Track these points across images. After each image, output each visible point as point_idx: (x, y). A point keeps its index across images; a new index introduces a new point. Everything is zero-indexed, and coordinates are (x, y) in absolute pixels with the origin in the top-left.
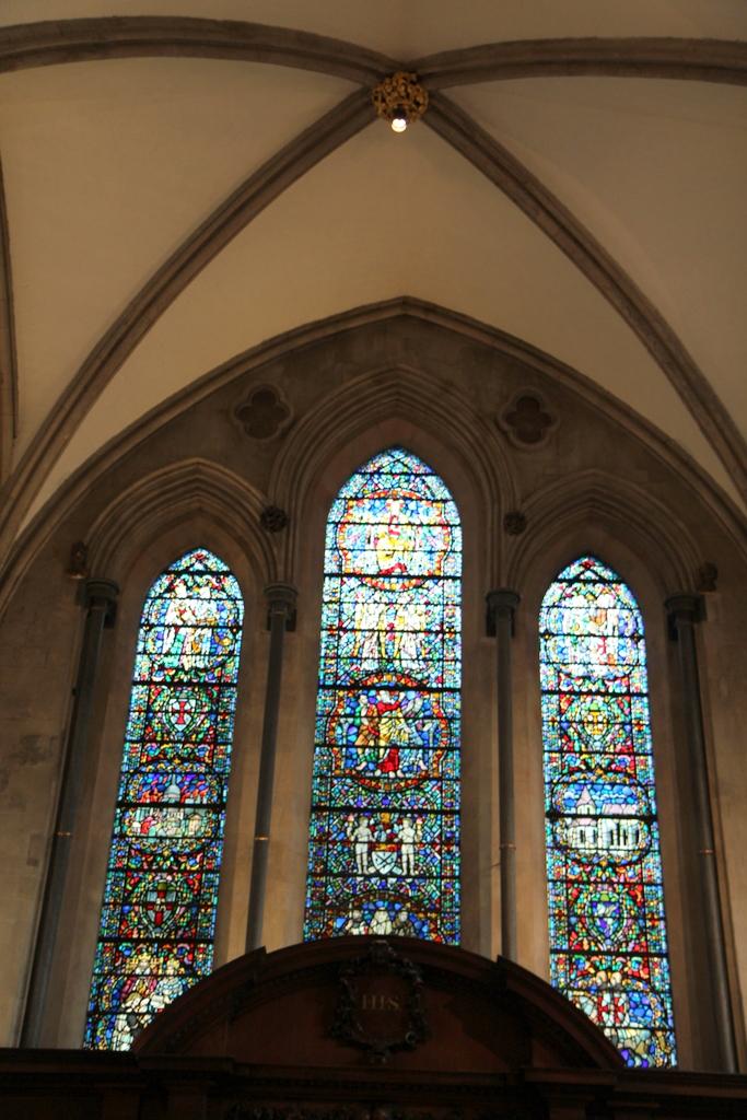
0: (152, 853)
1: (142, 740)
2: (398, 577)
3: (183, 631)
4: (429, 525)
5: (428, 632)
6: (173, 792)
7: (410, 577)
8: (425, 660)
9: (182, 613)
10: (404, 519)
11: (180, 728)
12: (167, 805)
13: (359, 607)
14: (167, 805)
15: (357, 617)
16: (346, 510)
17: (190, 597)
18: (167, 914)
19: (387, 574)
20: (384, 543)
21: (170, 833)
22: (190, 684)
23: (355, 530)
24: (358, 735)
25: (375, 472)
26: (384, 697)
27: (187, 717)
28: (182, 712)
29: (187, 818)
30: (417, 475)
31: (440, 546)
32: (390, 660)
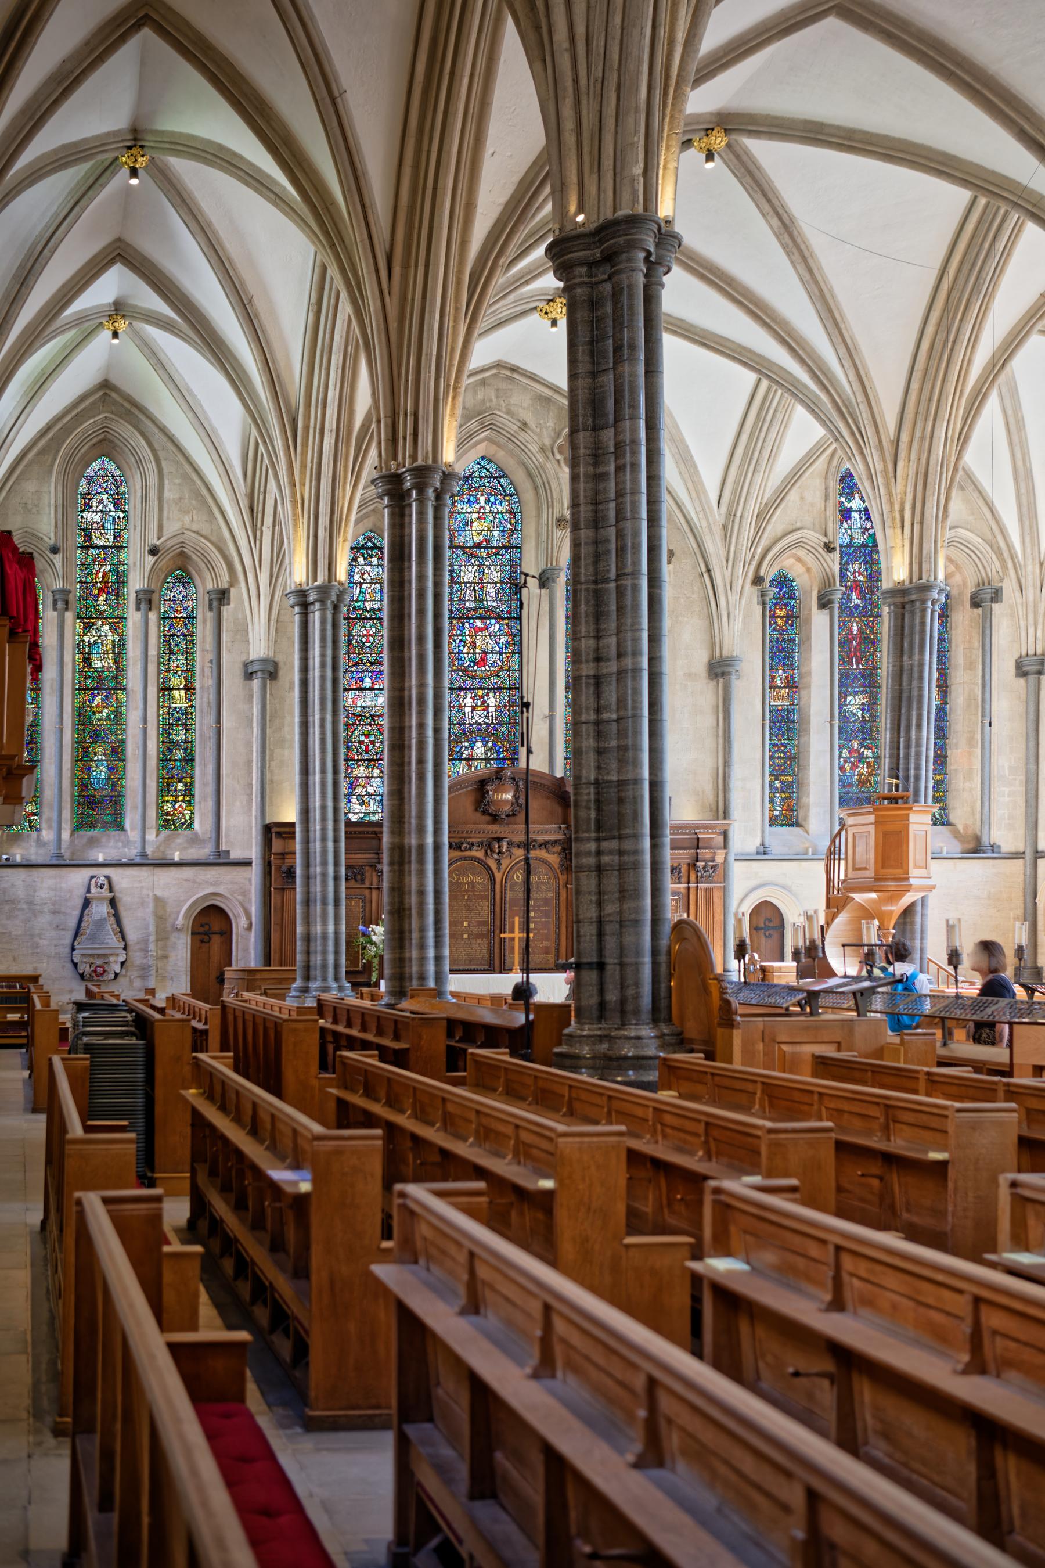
0: (360, 716)
1: (348, 653)
2: (486, 548)
3: (364, 586)
4: (502, 513)
5: (501, 582)
6: (368, 682)
7: (492, 548)
8: (500, 600)
9: (363, 574)
10: (488, 509)
11: (368, 644)
12: (366, 689)
13: (463, 568)
14: (366, 689)
15: (462, 574)
16: (453, 503)
17: (366, 564)
18: (371, 746)
19: (478, 546)
20: (475, 524)
21: (369, 704)
22: (371, 619)
23: (460, 518)
24: (464, 646)
25: (470, 476)
26: (478, 623)
27: (371, 639)
28: (368, 636)
29: (376, 696)
30: (495, 478)
31: (509, 526)
32: (481, 601)
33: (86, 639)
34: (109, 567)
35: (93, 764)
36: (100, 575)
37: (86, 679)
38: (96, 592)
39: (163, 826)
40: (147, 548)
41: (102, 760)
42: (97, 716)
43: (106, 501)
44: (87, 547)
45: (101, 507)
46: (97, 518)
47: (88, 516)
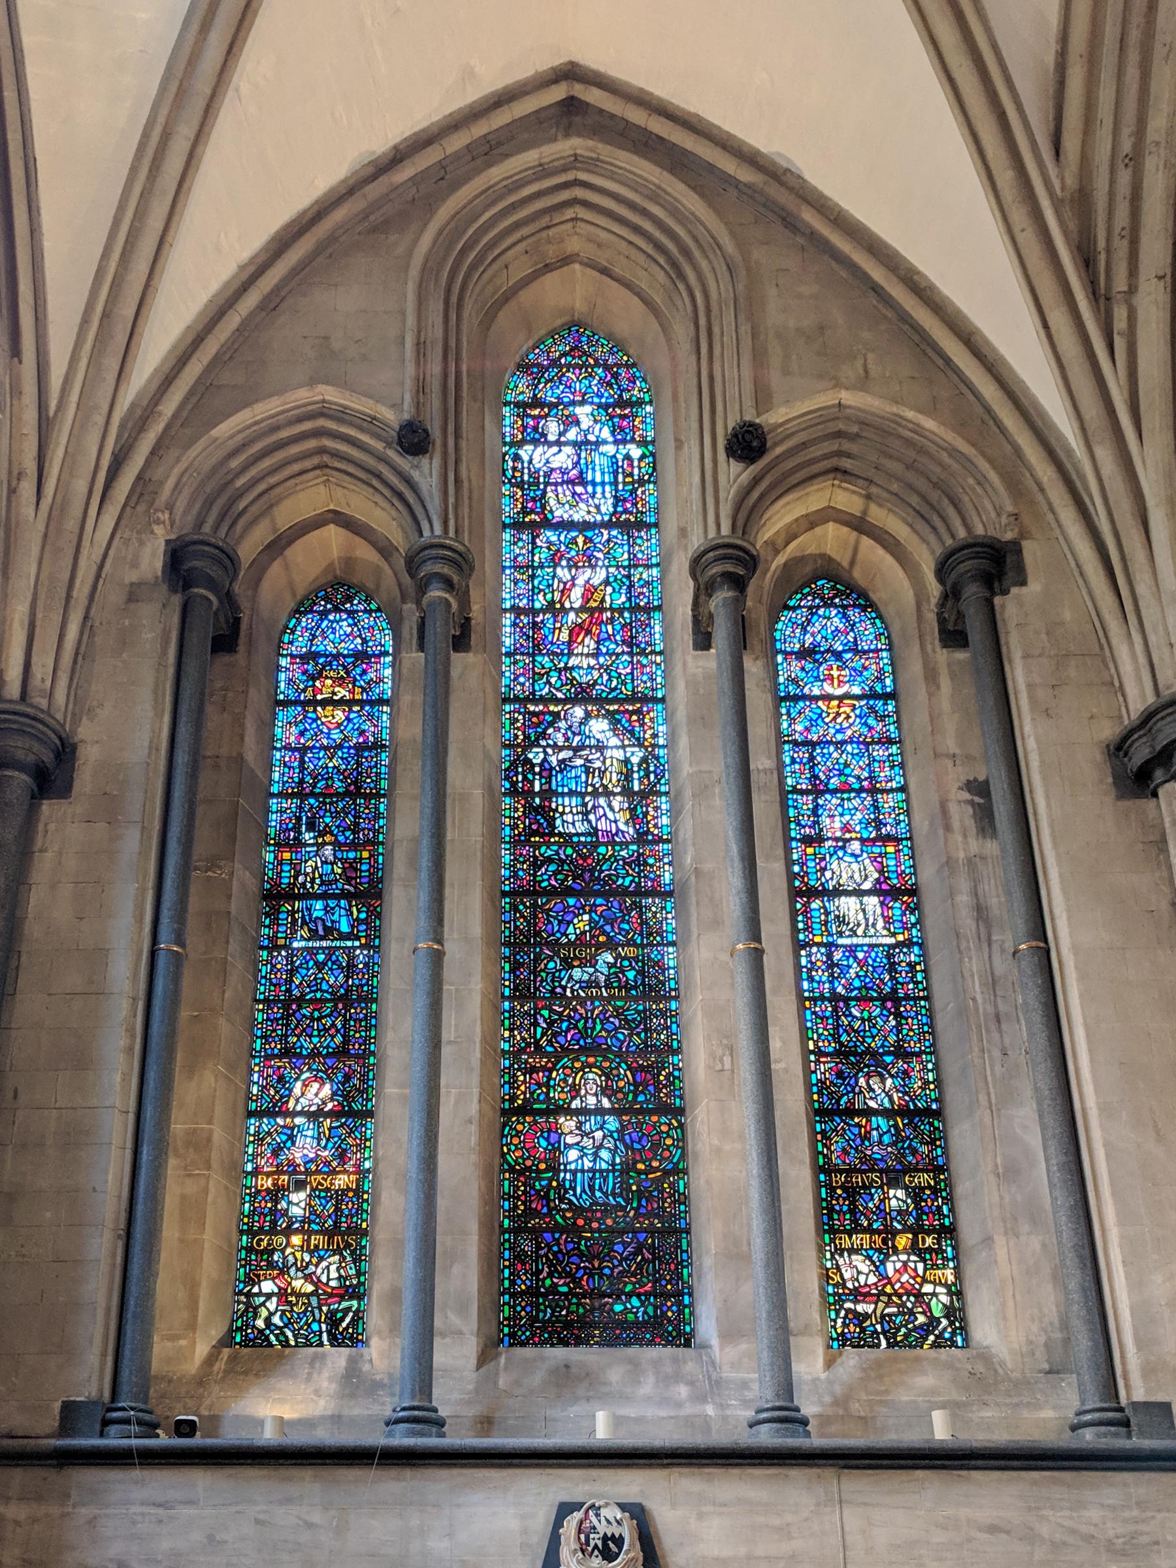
33: (536, 756)
34: (601, 575)
35: (568, 1124)
36: (576, 595)
37: (536, 864)
38: (565, 636)
39: (843, 1339)
40: (721, 444)
41: (599, 1111)
42: (577, 973)
43: (586, 423)
44: (535, 528)
45: (572, 435)
46: (563, 458)
47: (535, 456)
